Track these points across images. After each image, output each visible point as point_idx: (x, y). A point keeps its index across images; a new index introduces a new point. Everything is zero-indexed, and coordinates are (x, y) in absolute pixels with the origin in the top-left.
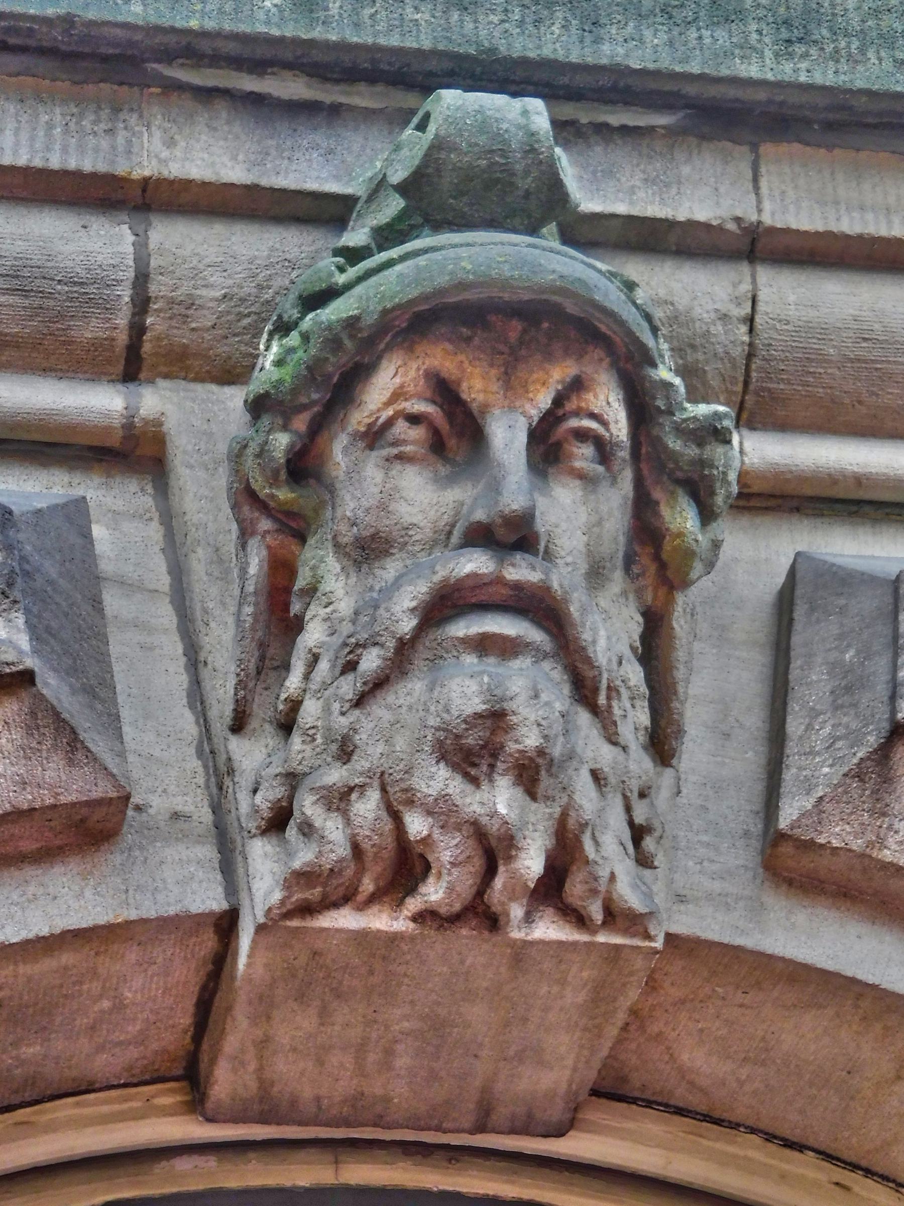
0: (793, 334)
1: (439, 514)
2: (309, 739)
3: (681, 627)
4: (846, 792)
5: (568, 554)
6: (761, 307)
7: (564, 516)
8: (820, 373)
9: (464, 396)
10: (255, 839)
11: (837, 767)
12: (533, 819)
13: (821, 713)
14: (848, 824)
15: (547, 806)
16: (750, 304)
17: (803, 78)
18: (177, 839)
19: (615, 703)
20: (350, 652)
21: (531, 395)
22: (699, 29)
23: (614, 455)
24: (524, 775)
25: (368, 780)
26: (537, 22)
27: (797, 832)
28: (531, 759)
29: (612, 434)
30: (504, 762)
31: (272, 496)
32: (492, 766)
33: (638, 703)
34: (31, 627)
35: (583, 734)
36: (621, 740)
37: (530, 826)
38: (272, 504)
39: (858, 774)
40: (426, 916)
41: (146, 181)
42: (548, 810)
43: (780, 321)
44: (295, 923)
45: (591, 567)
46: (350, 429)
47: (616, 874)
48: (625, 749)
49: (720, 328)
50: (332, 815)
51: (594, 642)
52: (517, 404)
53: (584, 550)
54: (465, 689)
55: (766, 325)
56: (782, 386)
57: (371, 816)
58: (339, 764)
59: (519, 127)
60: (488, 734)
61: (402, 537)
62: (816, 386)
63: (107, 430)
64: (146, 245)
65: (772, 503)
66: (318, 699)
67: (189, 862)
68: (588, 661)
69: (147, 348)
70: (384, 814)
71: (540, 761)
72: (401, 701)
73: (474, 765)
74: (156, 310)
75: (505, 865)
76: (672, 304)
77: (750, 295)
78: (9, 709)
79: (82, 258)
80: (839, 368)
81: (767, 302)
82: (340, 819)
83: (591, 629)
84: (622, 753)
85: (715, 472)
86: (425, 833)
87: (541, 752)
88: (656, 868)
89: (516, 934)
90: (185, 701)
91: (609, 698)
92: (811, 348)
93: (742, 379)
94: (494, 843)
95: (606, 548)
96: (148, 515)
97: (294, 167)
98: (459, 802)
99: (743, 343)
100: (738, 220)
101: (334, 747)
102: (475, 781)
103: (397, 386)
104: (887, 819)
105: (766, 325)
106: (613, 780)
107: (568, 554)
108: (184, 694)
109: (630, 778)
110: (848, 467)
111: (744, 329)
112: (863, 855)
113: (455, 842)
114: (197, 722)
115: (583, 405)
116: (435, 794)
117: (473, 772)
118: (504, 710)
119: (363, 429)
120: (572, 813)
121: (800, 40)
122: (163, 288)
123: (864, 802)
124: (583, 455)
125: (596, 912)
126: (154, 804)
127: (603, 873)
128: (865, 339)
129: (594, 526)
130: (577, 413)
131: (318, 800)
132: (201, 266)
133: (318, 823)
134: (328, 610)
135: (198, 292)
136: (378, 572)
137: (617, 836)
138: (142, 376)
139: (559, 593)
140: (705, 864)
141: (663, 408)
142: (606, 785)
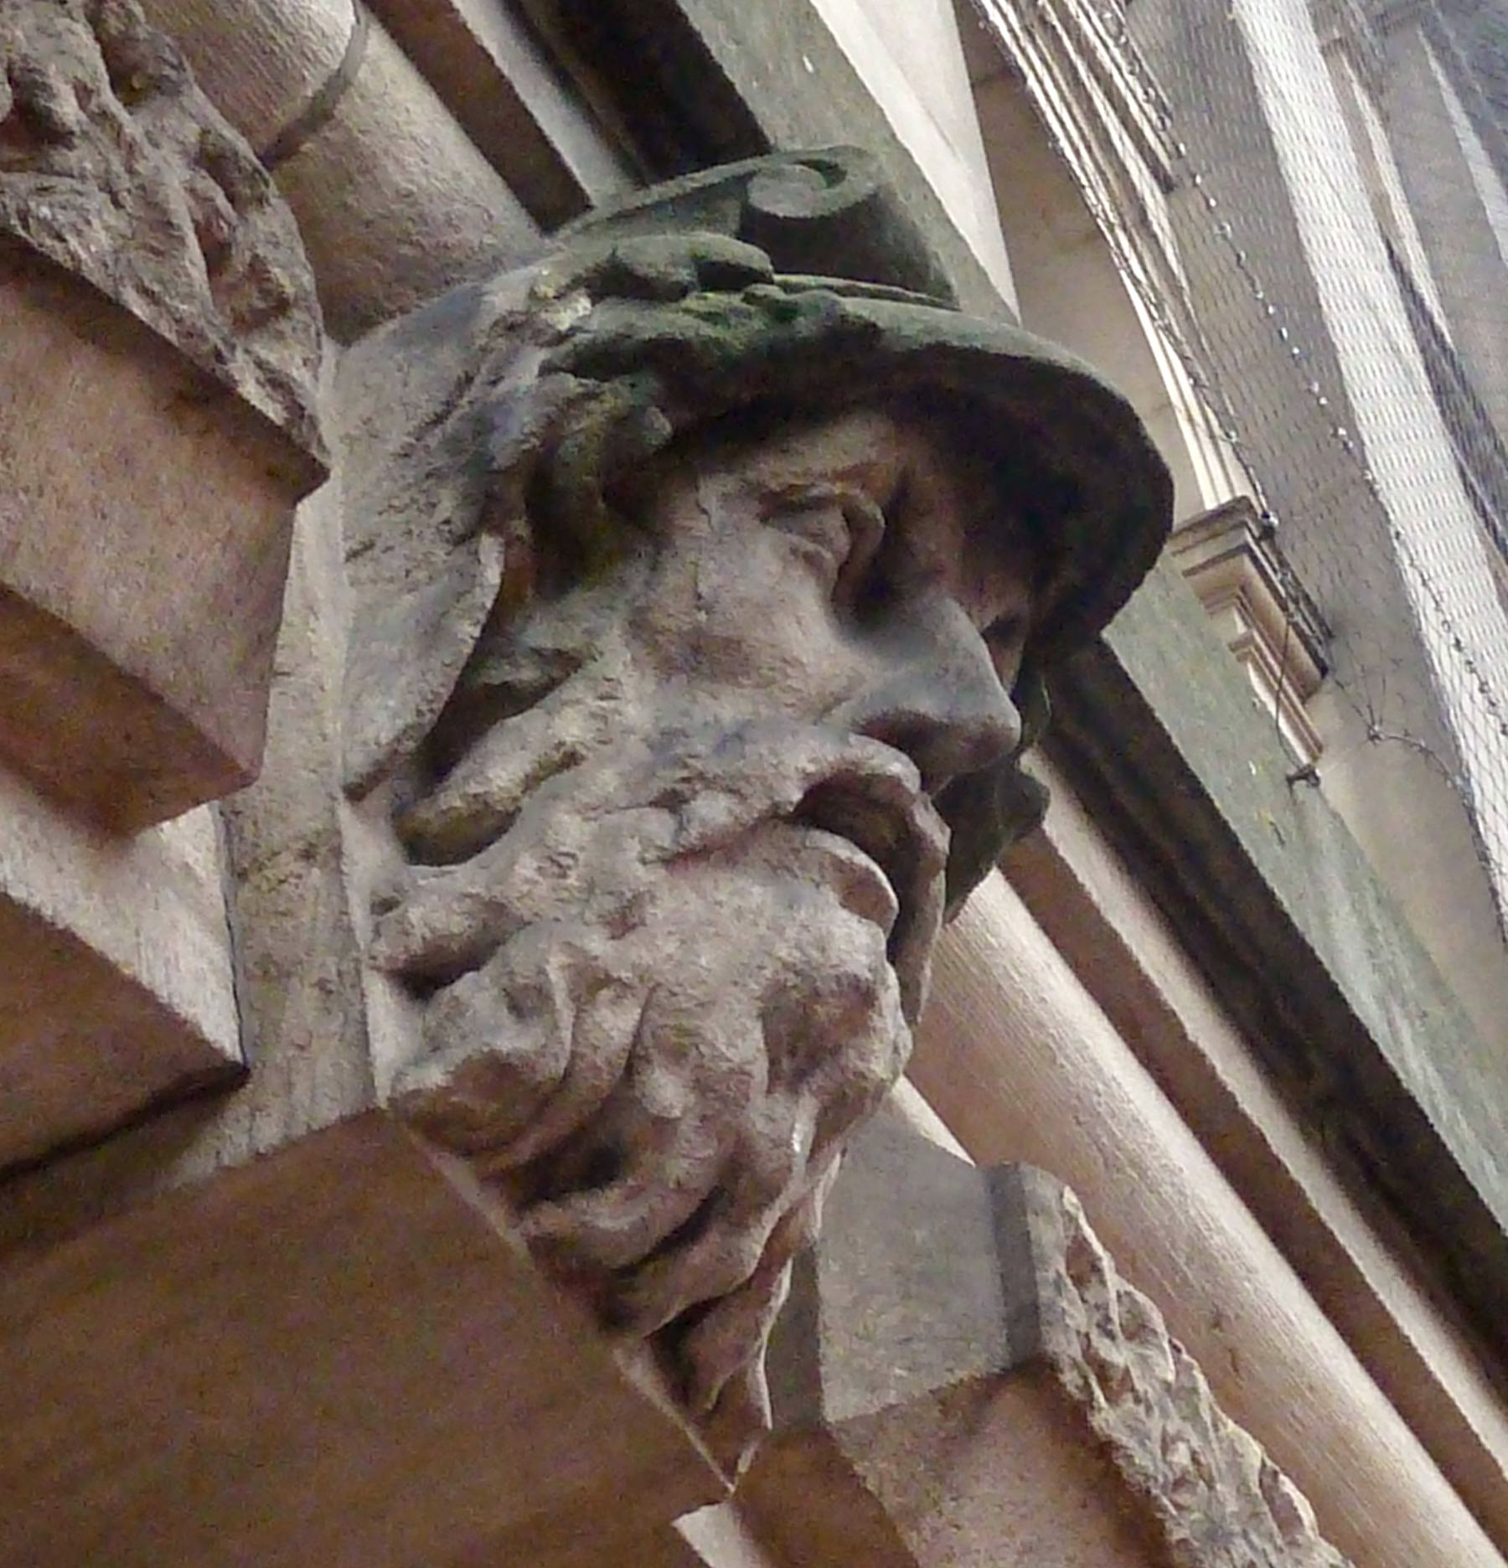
2: (556, 870)
20: (684, 780)
46: (751, 475)
58: (607, 932)
74: (326, 139)
75: (723, 1234)
86: (677, 1113)
116: (737, 1060)
119: (774, 486)
122: (355, 119)
131: (569, 966)
136: (702, 696)
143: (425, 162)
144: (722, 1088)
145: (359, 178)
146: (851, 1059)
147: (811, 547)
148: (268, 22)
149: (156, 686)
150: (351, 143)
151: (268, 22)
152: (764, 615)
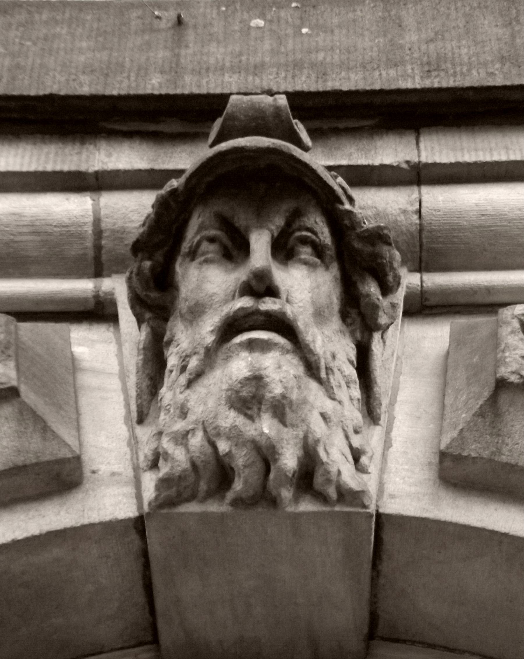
0: (443, 216)
1: (227, 286)
3: (377, 350)
4: (475, 425)
5: (300, 302)
6: (424, 204)
7: (296, 283)
8: (461, 236)
9: (237, 225)
10: (146, 473)
11: (469, 412)
12: (285, 437)
13: (461, 390)
14: (479, 443)
15: (294, 430)
16: (418, 204)
17: (436, 85)
18: (113, 485)
19: (331, 377)
20: (183, 361)
21: (271, 219)
22: (380, 71)
23: (325, 253)
24: (278, 412)
25: (196, 426)
26: (294, 77)
27: (450, 450)
28: (279, 401)
29: (320, 240)
30: (265, 405)
31: (146, 296)
32: (259, 409)
33: (352, 385)
34: (18, 368)
35: (313, 393)
36: (337, 397)
37: (285, 441)
38: (149, 301)
39: (481, 414)
40: (237, 502)
41: (96, 173)
42: (295, 433)
43: (435, 210)
44: (165, 511)
45: (316, 310)
46: (182, 253)
47: (341, 470)
48: (340, 402)
49: (403, 218)
50: (178, 447)
51: (314, 341)
52: (264, 225)
53: (310, 301)
54: (239, 366)
55: (427, 213)
56: (441, 245)
57: (198, 445)
58: (180, 420)
59: (270, 106)
60: (254, 390)
61: (210, 301)
62: (459, 244)
63: (86, 300)
64: (99, 204)
65: (445, 310)
66: (171, 390)
67: (119, 495)
68: (311, 351)
69: (104, 257)
70: (206, 444)
71: (284, 402)
72: (211, 382)
73: (249, 408)
76: (376, 208)
77: (418, 200)
78: (8, 410)
79: (65, 213)
80: (471, 232)
81: (427, 202)
82: (183, 449)
83: (312, 335)
84: (339, 405)
85: (385, 261)
86: (227, 450)
87: (284, 396)
88: (369, 473)
89: (290, 509)
90: (123, 421)
91: (327, 374)
92: (453, 223)
93: (418, 244)
94: (265, 451)
95: (323, 300)
96: (110, 340)
97: (172, 160)
98: (243, 429)
99: (416, 224)
100: (408, 162)
101: (178, 412)
102: (251, 418)
103: (200, 222)
104: (501, 438)
105: (427, 213)
106: (334, 419)
107: (300, 302)
108: (123, 418)
109: (346, 420)
110: (481, 283)
111: (415, 217)
112: (490, 460)
113: (243, 453)
114: (129, 431)
115: (302, 224)
117: (249, 412)
118: (261, 375)
120: (310, 435)
121: (435, 70)
122: (108, 224)
123: (486, 430)
124: (306, 253)
125: (332, 492)
126: (102, 469)
127: (333, 470)
128: (483, 215)
129: (314, 288)
130: (300, 229)
131: (170, 439)
132: (127, 212)
133: (170, 451)
134: (178, 348)
135: (127, 225)
137: (340, 450)
138: (104, 273)
139: (291, 316)
140: (406, 479)
141: (349, 225)
142: (330, 422)
143: (140, 213)
144: (231, 435)
145: (123, 236)
146: (268, 395)
147: (203, 258)
148: (64, 229)
149: (21, 464)
150: (113, 231)
151: (64, 229)
152: (199, 289)
